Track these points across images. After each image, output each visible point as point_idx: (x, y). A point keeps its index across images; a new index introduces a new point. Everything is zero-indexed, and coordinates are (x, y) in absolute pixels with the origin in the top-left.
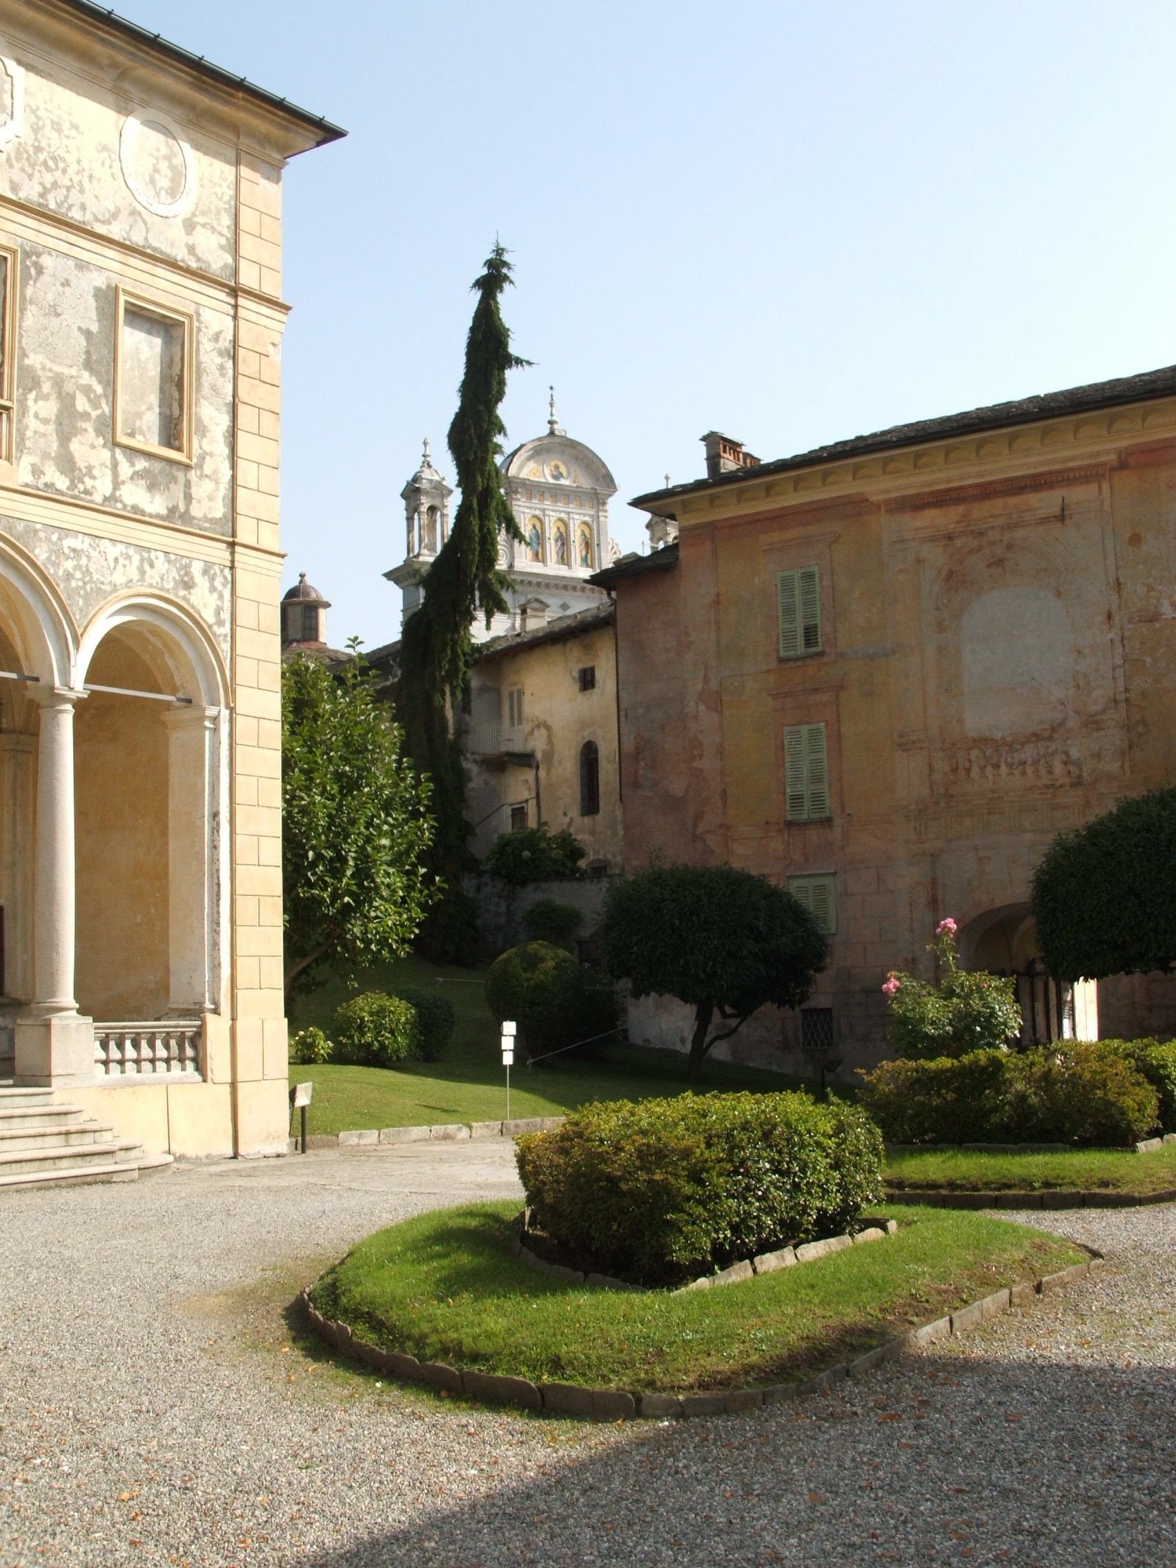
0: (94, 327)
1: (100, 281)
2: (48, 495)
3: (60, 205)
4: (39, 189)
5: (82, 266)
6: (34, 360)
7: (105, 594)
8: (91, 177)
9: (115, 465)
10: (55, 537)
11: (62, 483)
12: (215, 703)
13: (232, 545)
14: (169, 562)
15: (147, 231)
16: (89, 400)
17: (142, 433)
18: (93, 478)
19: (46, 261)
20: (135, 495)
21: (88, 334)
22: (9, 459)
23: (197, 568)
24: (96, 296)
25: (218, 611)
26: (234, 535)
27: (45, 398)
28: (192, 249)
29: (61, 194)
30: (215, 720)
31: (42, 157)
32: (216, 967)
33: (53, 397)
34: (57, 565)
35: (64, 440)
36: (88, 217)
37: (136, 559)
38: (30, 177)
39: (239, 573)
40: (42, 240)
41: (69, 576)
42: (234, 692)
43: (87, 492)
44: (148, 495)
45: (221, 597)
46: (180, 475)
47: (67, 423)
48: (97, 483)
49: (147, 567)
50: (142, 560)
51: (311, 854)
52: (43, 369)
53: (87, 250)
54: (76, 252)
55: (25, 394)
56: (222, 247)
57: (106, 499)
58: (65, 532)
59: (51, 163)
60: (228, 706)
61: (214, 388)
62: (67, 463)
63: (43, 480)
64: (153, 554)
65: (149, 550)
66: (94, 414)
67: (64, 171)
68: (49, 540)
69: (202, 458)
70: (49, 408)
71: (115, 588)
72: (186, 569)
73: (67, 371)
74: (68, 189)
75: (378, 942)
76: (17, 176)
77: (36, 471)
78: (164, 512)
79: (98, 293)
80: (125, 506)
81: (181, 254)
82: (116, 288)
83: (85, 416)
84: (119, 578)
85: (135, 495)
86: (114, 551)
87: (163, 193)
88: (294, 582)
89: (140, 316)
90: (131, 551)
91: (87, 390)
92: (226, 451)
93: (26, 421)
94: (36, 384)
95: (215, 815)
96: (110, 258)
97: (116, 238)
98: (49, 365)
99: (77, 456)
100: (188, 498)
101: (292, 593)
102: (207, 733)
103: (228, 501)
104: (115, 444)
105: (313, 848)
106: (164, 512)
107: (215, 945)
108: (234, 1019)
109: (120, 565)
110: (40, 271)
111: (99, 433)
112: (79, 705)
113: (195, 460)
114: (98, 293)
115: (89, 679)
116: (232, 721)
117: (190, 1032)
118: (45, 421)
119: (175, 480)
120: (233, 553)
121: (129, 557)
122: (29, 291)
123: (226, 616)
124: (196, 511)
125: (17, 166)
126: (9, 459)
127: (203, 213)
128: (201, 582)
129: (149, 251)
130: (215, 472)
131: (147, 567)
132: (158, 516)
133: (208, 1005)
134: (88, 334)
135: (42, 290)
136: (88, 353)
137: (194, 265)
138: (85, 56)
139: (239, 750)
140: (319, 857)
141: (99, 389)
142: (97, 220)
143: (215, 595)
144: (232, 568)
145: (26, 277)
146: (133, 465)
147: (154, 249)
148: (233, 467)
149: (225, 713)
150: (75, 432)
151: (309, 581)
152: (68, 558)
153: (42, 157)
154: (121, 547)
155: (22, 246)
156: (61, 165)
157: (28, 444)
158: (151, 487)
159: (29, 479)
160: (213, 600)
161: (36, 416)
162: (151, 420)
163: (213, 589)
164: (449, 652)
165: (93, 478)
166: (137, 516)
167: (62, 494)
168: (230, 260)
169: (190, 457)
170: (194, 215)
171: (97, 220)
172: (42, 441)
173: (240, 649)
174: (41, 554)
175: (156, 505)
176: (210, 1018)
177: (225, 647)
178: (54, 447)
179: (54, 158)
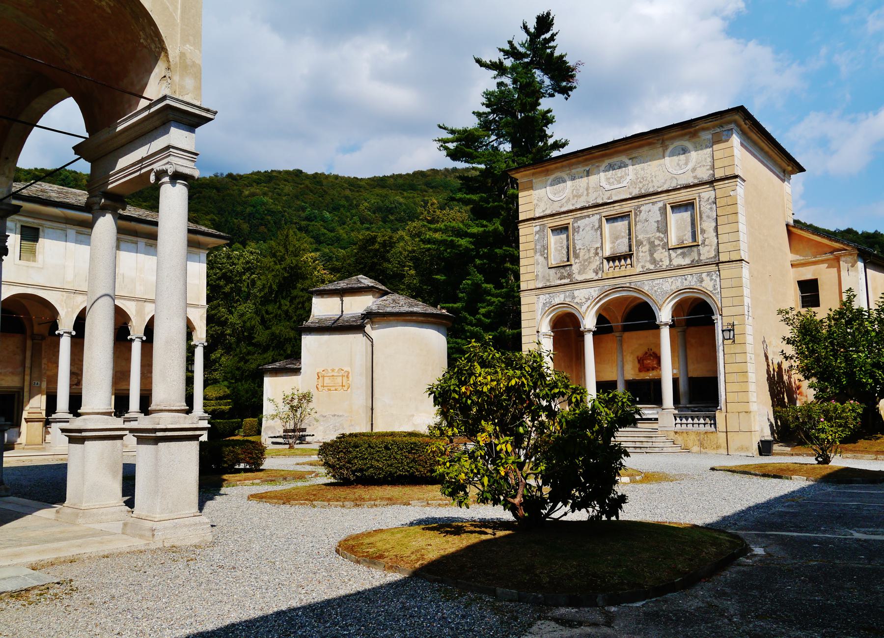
0: (659, 219)
1: (661, 204)
4: (638, 189)
6: (640, 237)
8: (655, 178)
9: (670, 255)
15: (677, 180)
16: (659, 240)
23: (704, 275)
24: (660, 210)
27: (645, 245)
28: (695, 177)
29: (645, 187)
35: (651, 255)
36: (656, 188)
37: (680, 280)
39: (721, 271)
44: (683, 260)
46: (695, 249)
53: (654, 199)
54: (651, 201)
56: (708, 170)
61: (708, 217)
62: (654, 261)
63: (645, 268)
66: (661, 244)
70: (646, 248)
73: (651, 236)
74: (648, 184)
76: (631, 190)
78: (690, 262)
81: (691, 181)
85: (678, 261)
86: (670, 280)
87: (683, 166)
93: (639, 254)
94: (642, 243)
96: (664, 197)
97: (665, 189)
98: (645, 236)
100: (699, 254)
109: (674, 284)
111: (663, 248)
120: (718, 266)
122: (637, 219)
127: (698, 163)
129: (679, 187)
131: (684, 281)
136: (658, 227)
137: (696, 181)
138: (650, 144)
141: (662, 236)
142: (658, 187)
143: (713, 281)
144: (719, 271)
146: (676, 253)
147: (680, 185)
152: (655, 287)
153: (638, 181)
159: (641, 270)
161: (642, 252)
163: (712, 280)
166: (680, 267)
168: (712, 172)
170: (696, 165)
171: (658, 187)
175: (687, 261)
178: (649, 258)
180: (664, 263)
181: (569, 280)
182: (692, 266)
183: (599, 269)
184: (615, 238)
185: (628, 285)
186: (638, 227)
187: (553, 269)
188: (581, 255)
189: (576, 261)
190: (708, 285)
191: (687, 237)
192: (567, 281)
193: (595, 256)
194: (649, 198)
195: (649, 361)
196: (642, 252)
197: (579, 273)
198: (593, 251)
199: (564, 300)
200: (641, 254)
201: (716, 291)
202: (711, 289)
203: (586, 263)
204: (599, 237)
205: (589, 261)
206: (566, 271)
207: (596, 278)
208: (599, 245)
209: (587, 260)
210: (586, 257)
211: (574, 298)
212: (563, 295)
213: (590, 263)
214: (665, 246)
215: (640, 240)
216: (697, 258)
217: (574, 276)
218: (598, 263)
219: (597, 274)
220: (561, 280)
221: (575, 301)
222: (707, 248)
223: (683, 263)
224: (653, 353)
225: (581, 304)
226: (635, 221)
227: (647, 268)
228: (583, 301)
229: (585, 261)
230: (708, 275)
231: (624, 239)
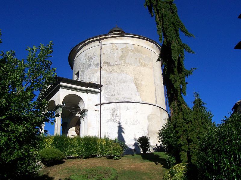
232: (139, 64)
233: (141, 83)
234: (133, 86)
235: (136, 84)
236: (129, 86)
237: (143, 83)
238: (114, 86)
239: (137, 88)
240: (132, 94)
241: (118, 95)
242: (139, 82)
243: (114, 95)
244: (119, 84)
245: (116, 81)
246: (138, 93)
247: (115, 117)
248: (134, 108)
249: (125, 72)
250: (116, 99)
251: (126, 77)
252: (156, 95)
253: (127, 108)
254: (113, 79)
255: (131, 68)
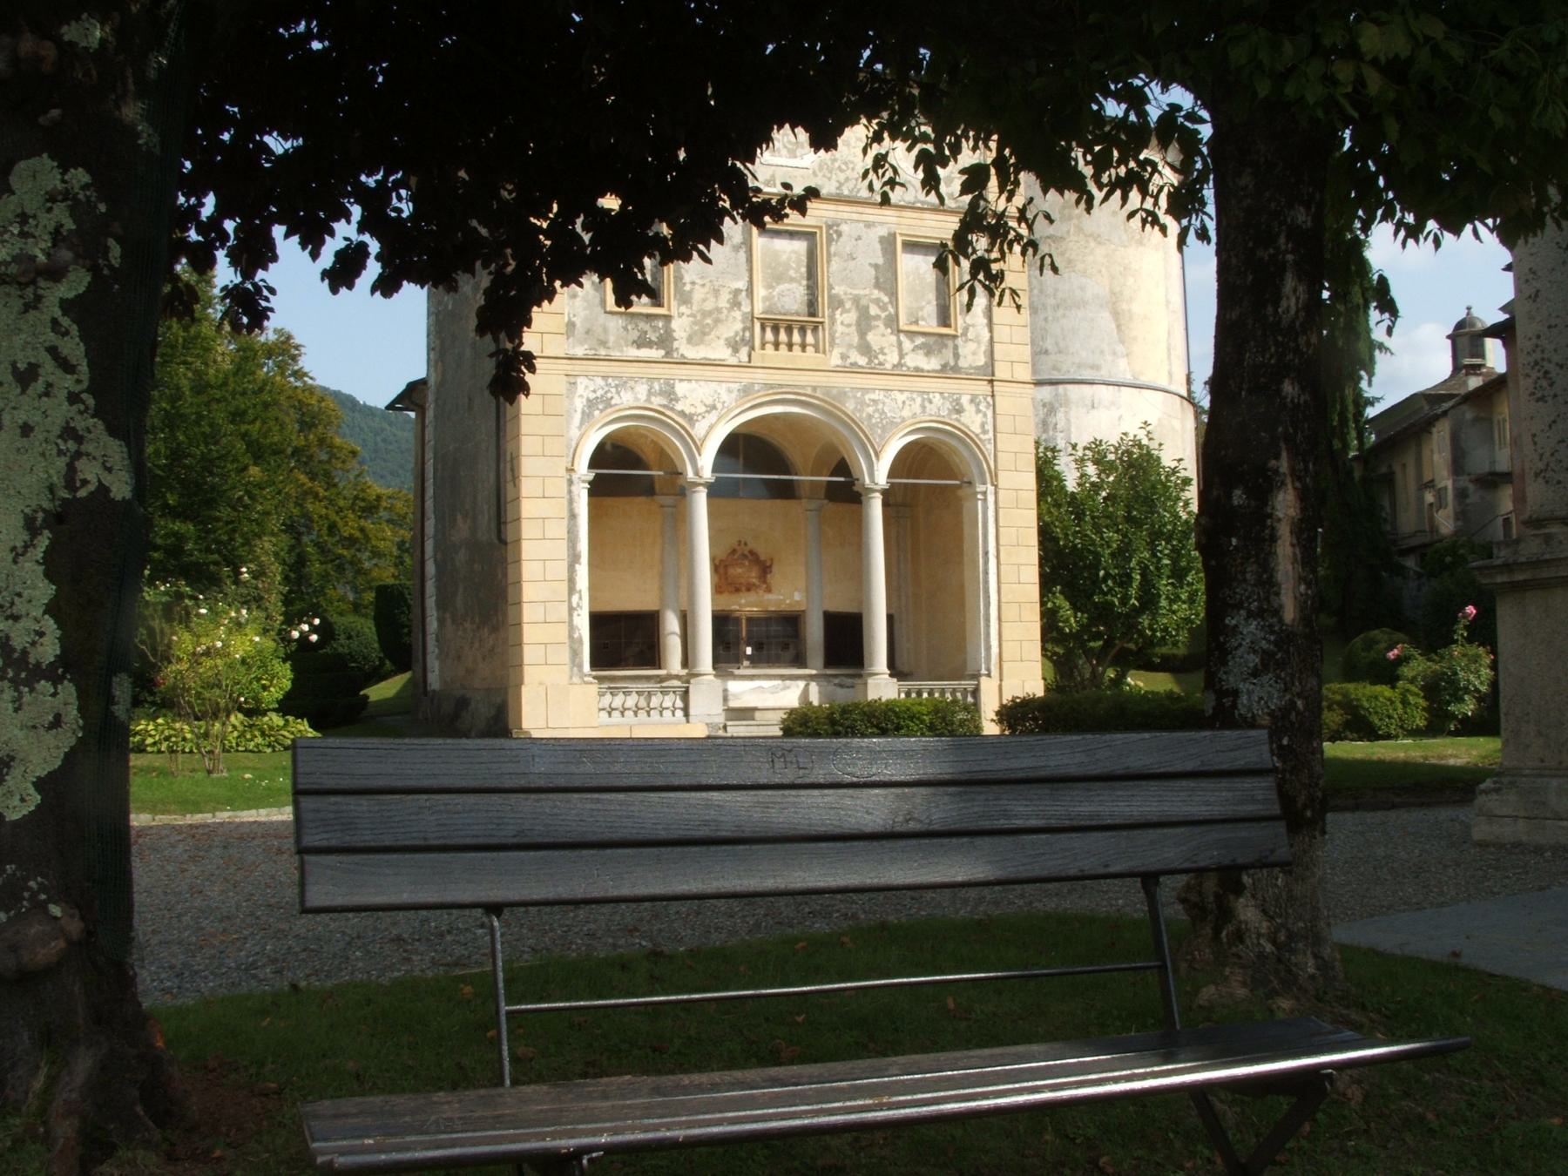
0: (880, 261)
1: (883, 232)
2: (854, 369)
3: (851, 191)
5: (869, 225)
6: (839, 290)
7: (897, 424)
9: (900, 344)
10: (859, 395)
11: (862, 361)
12: (984, 483)
13: (991, 381)
14: (944, 398)
17: (923, 319)
18: (884, 354)
19: (844, 228)
20: (916, 360)
21: (876, 266)
22: (824, 352)
23: (965, 400)
25: (983, 425)
26: (993, 375)
27: (848, 311)
30: (985, 493)
31: (837, 165)
32: (988, 648)
33: (854, 310)
34: (861, 411)
35: (862, 334)
37: (919, 400)
38: (829, 179)
40: (840, 215)
41: (870, 417)
42: (996, 475)
43: (880, 364)
44: (925, 359)
45: (985, 415)
46: (950, 343)
47: (864, 323)
48: (888, 358)
49: (927, 404)
50: (923, 400)
51: (1102, 573)
52: (845, 294)
54: (865, 217)
55: (833, 312)
57: (894, 366)
58: (866, 391)
59: (843, 167)
60: (993, 484)
62: (865, 349)
63: (849, 361)
64: (931, 396)
65: (928, 393)
66: (883, 315)
67: (853, 169)
68: (855, 397)
69: (966, 329)
70: (852, 317)
71: (904, 420)
72: (958, 402)
73: (862, 292)
75: (1162, 631)
77: (844, 357)
78: (939, 367)
79: (882, 240)
80: (909, 368)
82: (895, 234)
83: (877, 317)
84: (906, 413)
86: (901, 397)
88: (1462, 315)
89: (912, 246)
90: (915, 396)
91: (877, 301)
92: (985, 321)
95: (986, 553)
98: (849, 291)
99: (872, 343)
100: (956, 356)
101: (1460, 325)
102: (980, 503)
103: (988, 353)
104: (899, 331)
105: (1104, 569)
106: (939, 367)
107: (988, 635)
108: (1001, 680)
109: (907, 407)
110: (840, 234)
111: (887, 326)
112: (885, 493)
113: (960, 331)
114: (882, 240)
115: (892, 474)
116: (996, 493)
117: (970, 688)
118: (849, 326)
119: (946, 346)
121: (914, 400)
122: (833, 249)
123: (989, 427)
124: (963, 363)
125: (820, 175)
126: (824, 352)
128: (969, 408)
129: (919, 205)
130: (977, 336)
131: (927, 404)
132: (936, 371)
133: (984, 671)
134: (876, 266)
135: (843, 246)
136: (877, 278)
139: (1001, 512)
140: (1107, 575)
141: (886, 299)
143: (980, 415)
144: (993, 396)
145: (830, 240)
146: (913, 341)
148: (991, 331)
149: (991, 489)
150: (870, 328)
151: (1475, 313)
153: (837, 165)
154: (906, 394)
155: (826, 223)
156: (851, 166)
157: (837, 341)
158: (929, 353)
159: (839, 362)
160: (979, 419)
161: (842, 323)
162: (930, 310)
163: (978, 411)
164: (1338, 407)
165: (884, 354)
166: (918, 373)
167: (862, 367)
169: (956, 330)
172: (847, 338)
173: (1000, 446)
174: (850, 406)
175: (933, 364)
176: (983, 680)
177: (991, 447)
178: (856, 340)
179: (846, 163)
180: (888, 358)
181: (662, 352)
182: (950, 370)
183: (743, 339)
184: (777, 276)
185: (809, 391)
186: (835, 264)
187: (615, 317)
188: (698, 294)
189: (683, 309)
190: (972, 421)
191: (924, 313)
192: (656, 354)
193: (731, 309)
194: (860, 209)
195: (739, 570)
196: (842, 323)
197: (690, 340)
198: (725, 297)
199: (648, 400)
200: (839, 328)
201: (986, 437)
202: (978, 431)
203: (709, 321)
204: (744, 267)
205: (716, 316)
206: (655, 329)
207: (733, 361)
208: (742, 284)
209: (710, 313)
210: (709, 306)
211: (670, 394)
212: (646, 387)
213: (717, 321)
214: (892, 322)
215: (837, 296)
216: (952, 363)
217: (676, 344)
218: (739, 326)
219: (736, 350)
220: (639, 347)
221: (679, 407)
222: (972, 346)
223: (926, 367)
224: (751, 552)
225: (690, 418)
226: (828, 251)
227: (852, 360)
228: (699, 411)
229: (706, 314)
230: (972, 401)
231: (794, 285)
232: (1124, 237)
233: (1130, 311)
234: (1105, 320)
235: (1116, 315)
236: (1092, 320)
237: (1136, 308)
238: (1046, 320)
239: (1118, 326)
240: (1102, 352)
241: (1060, 352)
242: (1124, 306)
243: (1046, 352)
244: (1061, 312)
245: (1051, 301)
246: (1120, 348)
247: (1051, 433)
248: (1113, 403)
249: (1080, 266)
250: (1055, 368)
251: (1082, 288)
252: (1169, 350)
253: (1089, 403)
254: (1041, 291)
255: (1100, 252)
